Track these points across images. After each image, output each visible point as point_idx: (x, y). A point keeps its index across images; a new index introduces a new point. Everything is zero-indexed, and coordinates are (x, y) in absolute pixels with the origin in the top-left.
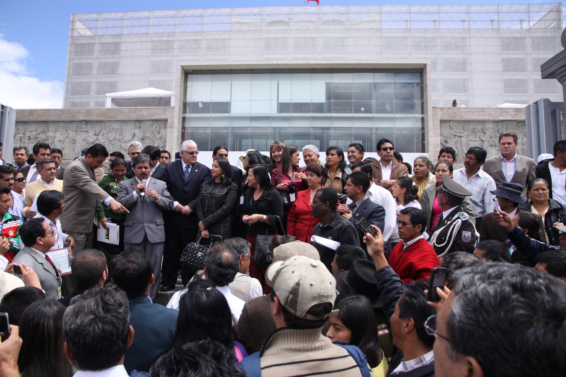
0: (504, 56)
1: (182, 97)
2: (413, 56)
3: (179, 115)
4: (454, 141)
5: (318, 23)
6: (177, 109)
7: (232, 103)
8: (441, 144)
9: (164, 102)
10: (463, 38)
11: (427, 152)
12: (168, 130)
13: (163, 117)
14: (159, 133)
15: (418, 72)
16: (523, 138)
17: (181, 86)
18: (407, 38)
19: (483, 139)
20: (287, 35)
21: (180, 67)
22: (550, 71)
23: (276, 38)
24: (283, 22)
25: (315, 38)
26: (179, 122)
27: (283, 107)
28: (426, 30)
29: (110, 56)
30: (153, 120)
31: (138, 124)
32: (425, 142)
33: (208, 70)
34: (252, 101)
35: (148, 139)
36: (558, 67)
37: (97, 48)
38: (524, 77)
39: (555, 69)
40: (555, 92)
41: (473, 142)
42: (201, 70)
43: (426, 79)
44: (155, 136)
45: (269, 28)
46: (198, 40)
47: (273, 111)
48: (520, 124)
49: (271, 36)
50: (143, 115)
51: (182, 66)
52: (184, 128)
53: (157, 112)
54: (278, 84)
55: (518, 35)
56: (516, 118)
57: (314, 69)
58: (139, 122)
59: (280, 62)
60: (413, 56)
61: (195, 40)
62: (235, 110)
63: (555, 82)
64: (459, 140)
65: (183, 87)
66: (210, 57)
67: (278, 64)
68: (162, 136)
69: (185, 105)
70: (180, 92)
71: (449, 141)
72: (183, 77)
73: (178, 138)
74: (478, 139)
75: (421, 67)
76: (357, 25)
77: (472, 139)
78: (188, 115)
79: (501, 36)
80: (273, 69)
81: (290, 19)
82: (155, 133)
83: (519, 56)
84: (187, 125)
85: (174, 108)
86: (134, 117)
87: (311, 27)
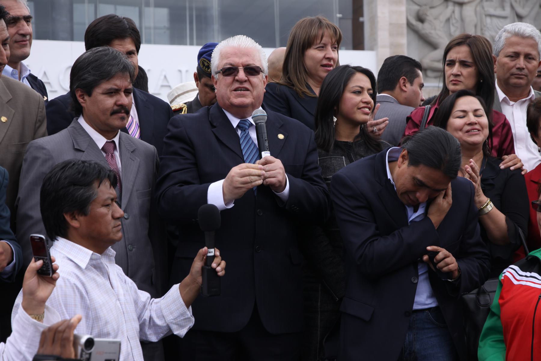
4: (443, 18)
8: (409, 25)
11: (372, 49)
19: (521, 11)
32: (365, 19)
41: (495, 20)
64: (457, 14)
71: (431, 14)
74: (507, 11)
77: (492, 11)
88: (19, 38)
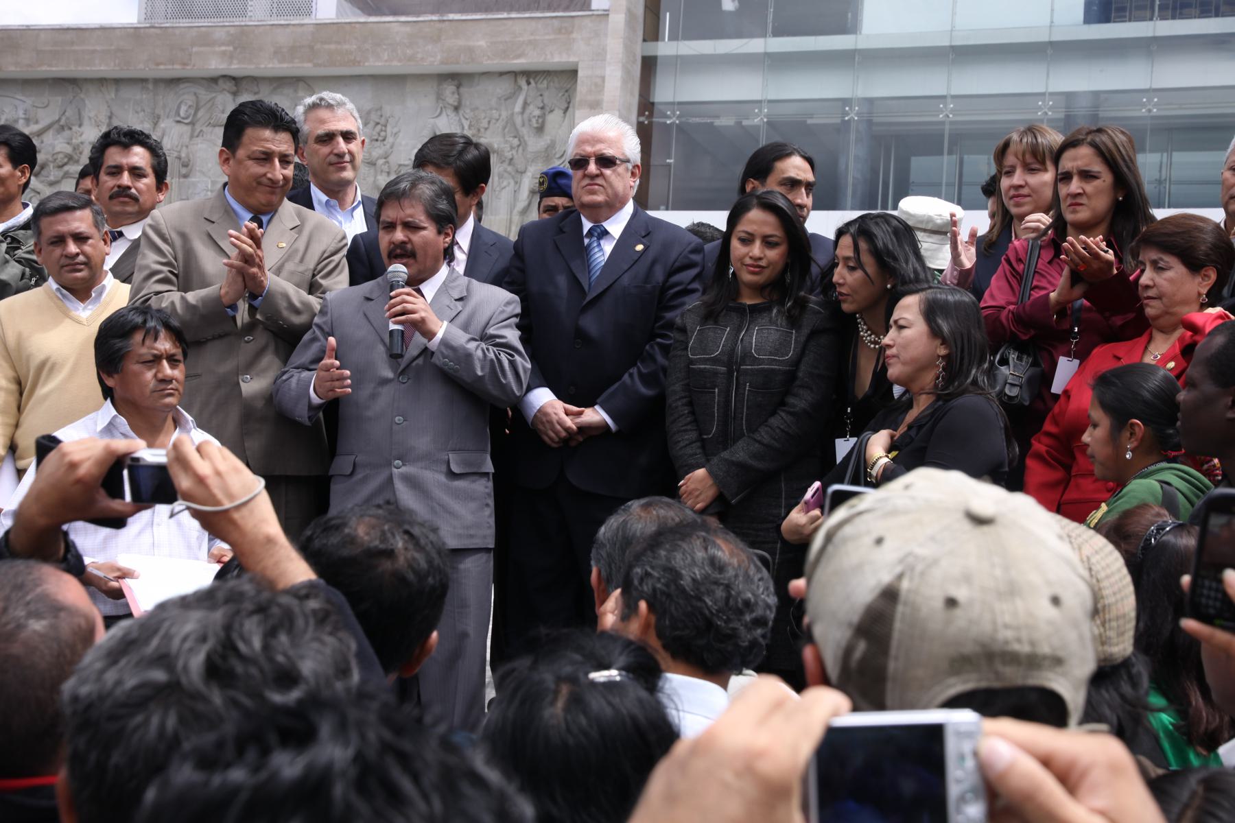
3: (628, 48)
6: (618, 20)
13: (557, 58)
14: (540, 129)
26: (625, 82)
30: (515, 74)
31: (449, 89)
44: (522, 144)
50: (471, 50)
52: (646, 106)
58: (457, 79)
68: (552, 145)
78: (665, 48)
82: (524, 131)
84: (663, 93)
85: (605, 15)
86: (433, 59)
88: (333, 159)
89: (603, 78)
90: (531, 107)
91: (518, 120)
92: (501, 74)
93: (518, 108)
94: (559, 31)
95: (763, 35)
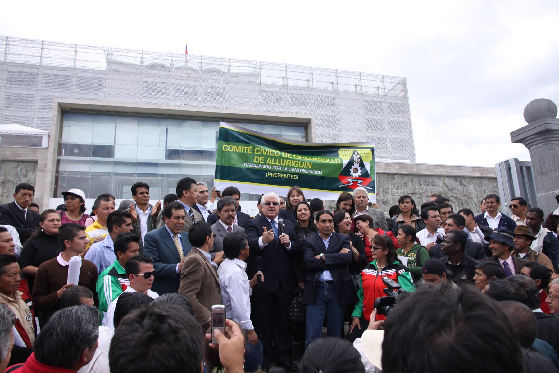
0: (368, 117)
1: (58, 137)
2: (290, 110)
3: (54, 157)
5: (200, 72)
6: (51, 150)
7: (116, 147)
9: (34, 142)
10: (333, 97)
12: (38, 173)
13: (32, 158)
14: (26, 176)
15: (302, 126)
16: (392, 189)
17: (57, 126)
18: (284, 93)
20: (168, 81)
21: (56, 106)
22: (518, 137)
23: (156, 83)
24: (163, 67)
25: (196, 86)
26: (53, 165)
27: (173, 154)
28: (301, 89)
29: (59, 90)
30: (18, 161)
33: (90, 110)
34: (137, 145)
35: (10, 183)
36: (528, 135)
37: (40, 79)
38: (383, 136)
39: (526, 136)
40: (522, 153)
42: (80, 110)
43: (311, 133)
45: (148, 71)
46: (69, 76)
47: (161, 157)
48: (390, 177)
49: (150, 80)
50: (5, 155)
51: (60, 104)
52: (57, 172)
53: (26, 154)
54: (167, 129)
55: (376, 99)
56: (387, 171)
57: (204, 117)
59: (170, 108)
60: (290, 110)
61: (65, 76)
62: (119, 155)
63: (521, 146)
65: (59, 127)
66: (82, 96)
67: (168, 110)
69: (60, 146)
70: (56, 131)
72: (60, 115)
73: (51, 183)
75: (306, 122)
76: (237, 77)
78: (63, 158)
79: (364, 99)
80: (162, 114)
81: (170, 65)
82: (21, 176)
83: (379, 118)
84: (62, 168)
85: (47, 149)
87: (193, 74)
89: (46, 165)
90: (23, 171)
91: (19, 173)
92: (14, 161)
93: (19, 170)
94: (33, 151)
95: (90, 156)
